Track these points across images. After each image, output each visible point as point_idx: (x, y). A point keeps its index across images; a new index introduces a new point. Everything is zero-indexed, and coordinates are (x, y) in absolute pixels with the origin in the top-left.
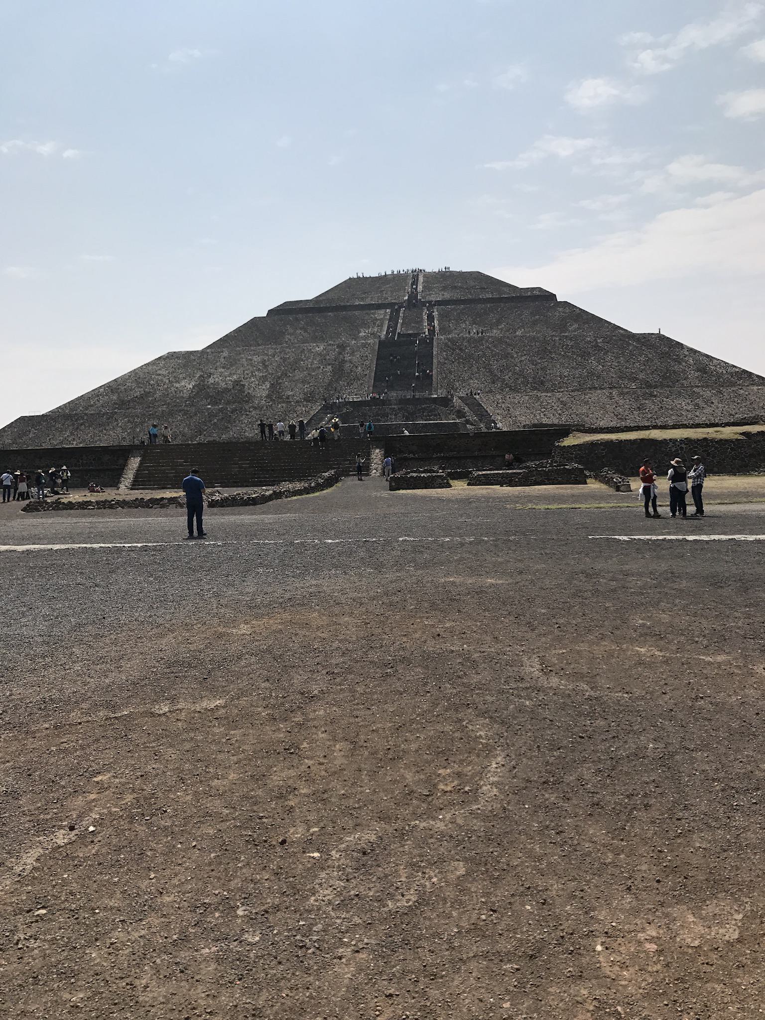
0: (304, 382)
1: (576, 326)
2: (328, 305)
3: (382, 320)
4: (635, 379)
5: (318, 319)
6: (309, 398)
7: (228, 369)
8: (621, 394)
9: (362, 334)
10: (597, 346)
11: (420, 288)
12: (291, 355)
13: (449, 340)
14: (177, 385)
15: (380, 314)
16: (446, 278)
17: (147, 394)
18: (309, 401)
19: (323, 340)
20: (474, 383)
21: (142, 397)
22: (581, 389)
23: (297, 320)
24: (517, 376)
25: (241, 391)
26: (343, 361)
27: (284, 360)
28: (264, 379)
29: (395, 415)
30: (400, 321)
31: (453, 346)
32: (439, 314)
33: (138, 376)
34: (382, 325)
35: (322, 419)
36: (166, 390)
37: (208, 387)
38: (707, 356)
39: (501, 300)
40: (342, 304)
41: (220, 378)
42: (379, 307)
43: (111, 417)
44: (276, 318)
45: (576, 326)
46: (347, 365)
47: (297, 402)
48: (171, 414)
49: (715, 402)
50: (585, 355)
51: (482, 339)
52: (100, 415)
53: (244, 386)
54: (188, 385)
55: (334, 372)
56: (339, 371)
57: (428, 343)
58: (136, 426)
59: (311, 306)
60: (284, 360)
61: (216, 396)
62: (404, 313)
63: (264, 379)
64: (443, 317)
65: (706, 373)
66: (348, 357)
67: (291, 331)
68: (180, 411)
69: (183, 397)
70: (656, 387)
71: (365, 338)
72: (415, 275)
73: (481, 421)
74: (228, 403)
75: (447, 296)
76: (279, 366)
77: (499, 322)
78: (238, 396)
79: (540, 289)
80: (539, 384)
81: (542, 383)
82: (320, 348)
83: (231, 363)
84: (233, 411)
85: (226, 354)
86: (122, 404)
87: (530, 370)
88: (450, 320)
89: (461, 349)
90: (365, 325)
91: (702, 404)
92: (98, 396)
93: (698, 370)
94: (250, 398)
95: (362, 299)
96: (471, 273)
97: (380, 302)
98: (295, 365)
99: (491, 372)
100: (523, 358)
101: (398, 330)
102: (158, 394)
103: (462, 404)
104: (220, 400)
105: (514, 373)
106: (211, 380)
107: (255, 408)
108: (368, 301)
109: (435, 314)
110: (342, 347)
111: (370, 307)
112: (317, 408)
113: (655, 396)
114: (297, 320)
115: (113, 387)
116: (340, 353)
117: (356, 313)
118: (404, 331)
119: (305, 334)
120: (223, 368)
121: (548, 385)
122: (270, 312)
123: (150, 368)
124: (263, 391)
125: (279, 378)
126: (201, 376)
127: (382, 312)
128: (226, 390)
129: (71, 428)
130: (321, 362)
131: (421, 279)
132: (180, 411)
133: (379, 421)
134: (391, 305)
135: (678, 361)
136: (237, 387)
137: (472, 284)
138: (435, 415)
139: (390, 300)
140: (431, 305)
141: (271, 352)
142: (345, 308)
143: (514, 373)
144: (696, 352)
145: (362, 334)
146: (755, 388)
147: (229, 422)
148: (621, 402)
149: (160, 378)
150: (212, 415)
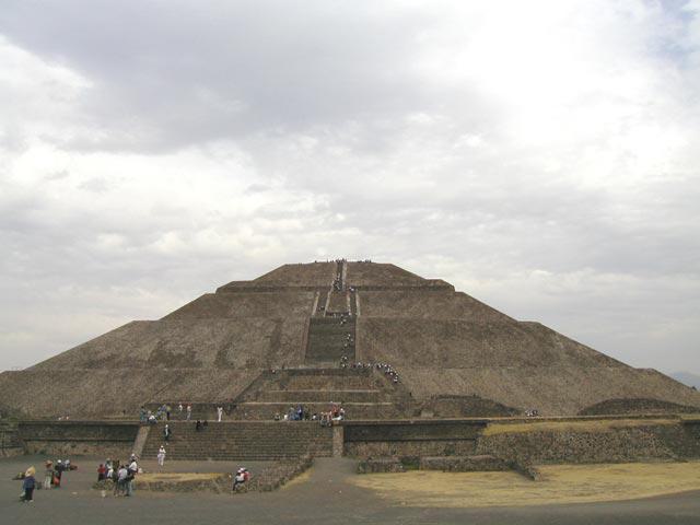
1: (470, 313)
3: (313, 301)
4: (519, 359)
6: (250, 365)
9: (296, 311)
11: (345, 274)
13: (369, 320)
15: (310, 295)
21: (109, 359)
25: (193, 357)
30: (328, 301)
31: (373, 326)
38: (575, 342)
42: (310, 289)
44: (224, 294)
49: (583, 379)
50: (479, 338)
51: (396, 321)
54: (147, 350)
56: (275, 343)
57: (353, 320)
58: (102, 385)
59: (254, 285)
61: (171, 360)
63: (212, 347)
66: (284, 331)
71: (298, 315)
72: (340, 263)
75: (367, 283)
77: (408, 306)
78: (190, 360)
79: (442, 281)
80: (446, 361)
81: (446, 360)
86: (92, 364)
91: (571, 379)
93: (567, 353)
94: (200, 364)
96: (385, 265)
108: (301, 284)
109: (357, 296)
110: (279, 321)
115: (86, 348)
121: (450, 361)
122: (219, 290)
124: (212, 357)
125: (226, 347)
128: (180, 356)
131: (345, 268)
133: (311, 388)
134: (317, 288)
135: (552, 345)
145: (296, 311)
146: (611, 370)
147: (181, 383)
150: (167, 377)
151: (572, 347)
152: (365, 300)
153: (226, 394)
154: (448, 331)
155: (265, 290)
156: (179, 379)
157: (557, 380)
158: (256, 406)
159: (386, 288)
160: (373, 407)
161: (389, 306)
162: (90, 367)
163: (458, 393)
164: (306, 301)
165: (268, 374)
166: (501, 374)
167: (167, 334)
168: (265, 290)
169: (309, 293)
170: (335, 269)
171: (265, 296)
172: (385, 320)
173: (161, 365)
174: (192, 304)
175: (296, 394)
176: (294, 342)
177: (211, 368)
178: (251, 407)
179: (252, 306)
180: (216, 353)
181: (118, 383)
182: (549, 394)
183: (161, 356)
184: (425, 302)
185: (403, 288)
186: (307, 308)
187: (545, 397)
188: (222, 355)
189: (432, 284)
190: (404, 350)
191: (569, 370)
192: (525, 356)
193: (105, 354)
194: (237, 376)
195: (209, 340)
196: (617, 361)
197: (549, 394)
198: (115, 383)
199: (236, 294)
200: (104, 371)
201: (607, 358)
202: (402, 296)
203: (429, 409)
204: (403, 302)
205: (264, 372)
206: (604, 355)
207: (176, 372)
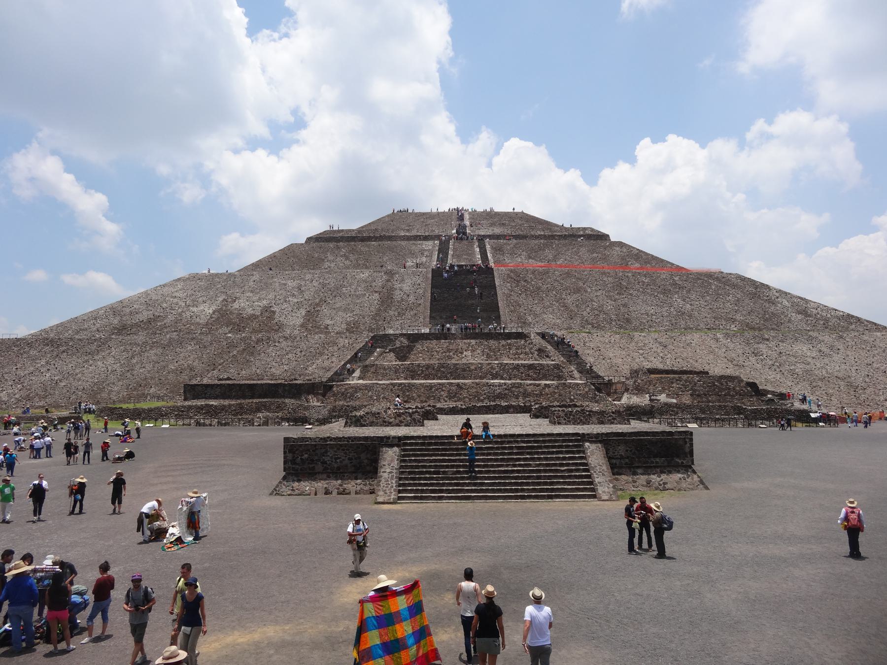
0: (345, 310)
2: (372, 235)
4: (734, 321)
5: (360, 246)
6: (352, 328)
7: (257, 293)
8: (727, 336)
9: (409, 264)
10: (675, 284)
12: (331, 282)
13: (511, 271)
14: (195, 309)
15: (428, 245)
16: (491, 216)
17: (156, 318)
18: (353, 332)
19: (367, 268)
20: (549, 317)
21: (149, 321)
22: (674, 326)
24: (596, 312)
25: (271, 317)
26: (392, 289)
27: (324, 285)
28: (299, 305)
29: (473, 351)
30: (451, 252)
31: (516, 277)
32: (492, 248)
33: (148, 300)
35: (371, 353)
36: (180, 315)
37: (231, 313)
39: (552, 237)
40: (387, 234)
41: (247, 304)
42: (426, 238)
43: (103, 344)
45: (637, 265)
46: (397, 292)
47: (337, 333)
48: (180, 343)
52: (91, 341)
53: (274, 312)
54: (206, 310)
55: (382, 302)
56: (387, 299)
58: (133, 357)
61: (239, 322)
62: (453, 245)
63: (299, 305)
64: (497, 250)
65: (810, 316)
66: (397, 286)
67: (331, 258)
68: (193, 339)
69: (198, 324)
70: (760, 330)
73: (570, 362)
74: (254, 331)
75: (497, 231)
76: (316, 292)
77: (555, 258)
78: (267, 323)
79: (592, 230)
80: (625, 323)
81: (628, 321)
82: (365, 274)
83: (264, 286)
84: (258, 341)
85: (256, 277)
86: (122, 329)
87: (609, 306)
88: (503, 255)
89: (525, 281)
90: (413, 254)
93: (800, 313)
94: (280, 327)
95: (408, 230)
97: (427, 234)
98: (336, 291)
99: (565, 306)
101: (449, 261)
102: (171, 318)
103: (544, 343)
104: (244, 328)
105: (593, 309)
106: (236, 305)
107: (286, 338)
108: (414, 233)
109: (488, 247)
110: (391, 274)
111: (416, 238)
112: (364, 338)
113: (768, 340)
114: (338, 248)
115: (115, 310)
116: (388, 281)
117: (403, 243)
118: (455, 262)
119: (348, 263)
121: (635, 323)
122: (309, 240)
123: (167, 288)
125: (317, 305)
127: (430, 243)
128: (253, 317)
129: (49, 356)
130: (367, 289)
131: (467, 216)
132: (193, 339)
133: (450, 358)
134: (438, 237)
136: (267, 314)
137: (520, 222)
138: (526, 353)
139: (437, 232)
140: (481, 239)
141: (308, 277)
142: (390, 238)
143: (593, 309)
144: (786, 293)
147: (252, 354)
148: (731, 346)
149: (175, 300)
150: (231, 345)
151: (802, 307)
153: (318, 370)
154: (620, 287)
155: (369, 239)
156: (250, 350)
157: (802, 348)
158: (366, 386)
159: (524, 237)
160: (557, 387)
161: (530, 258)
162: (116, 334)
163: (661, 366)
164: (422, 252)
165: (380, 341)
166: (717, 340)
167: (237, 292)
168: (369, 239)
170: (455, 217)
171: (368, 246)
172: (533, 272)
173: (225, 329)
174: (273, 257)
175: (428, 367)
176: (412, 299)
177: (296, 332)
178: (357, 388)
179: (352, 257)
180: (303, 312)
181: (156, 354)
182: (799, 368)
183: (223, 317)
184: (577, 253)
185: (545, 237)
186: (424, 259)
187: (792, 373)
189: (581, 233)
191: (814, 334)
192: (738, 317)
193: (145, 316)
194: (335, 344)
195: (294, 295)
196: (875, 324)
197: (799, 368)
198: (152, 354)
199: (331, 245)
200: (141, 337)
201: (859, 320)
202: (546, 246)
203: (639, 390)
204: (549, 253)
205: (372, 337)
206: (853, 316)
207: (243, 339)
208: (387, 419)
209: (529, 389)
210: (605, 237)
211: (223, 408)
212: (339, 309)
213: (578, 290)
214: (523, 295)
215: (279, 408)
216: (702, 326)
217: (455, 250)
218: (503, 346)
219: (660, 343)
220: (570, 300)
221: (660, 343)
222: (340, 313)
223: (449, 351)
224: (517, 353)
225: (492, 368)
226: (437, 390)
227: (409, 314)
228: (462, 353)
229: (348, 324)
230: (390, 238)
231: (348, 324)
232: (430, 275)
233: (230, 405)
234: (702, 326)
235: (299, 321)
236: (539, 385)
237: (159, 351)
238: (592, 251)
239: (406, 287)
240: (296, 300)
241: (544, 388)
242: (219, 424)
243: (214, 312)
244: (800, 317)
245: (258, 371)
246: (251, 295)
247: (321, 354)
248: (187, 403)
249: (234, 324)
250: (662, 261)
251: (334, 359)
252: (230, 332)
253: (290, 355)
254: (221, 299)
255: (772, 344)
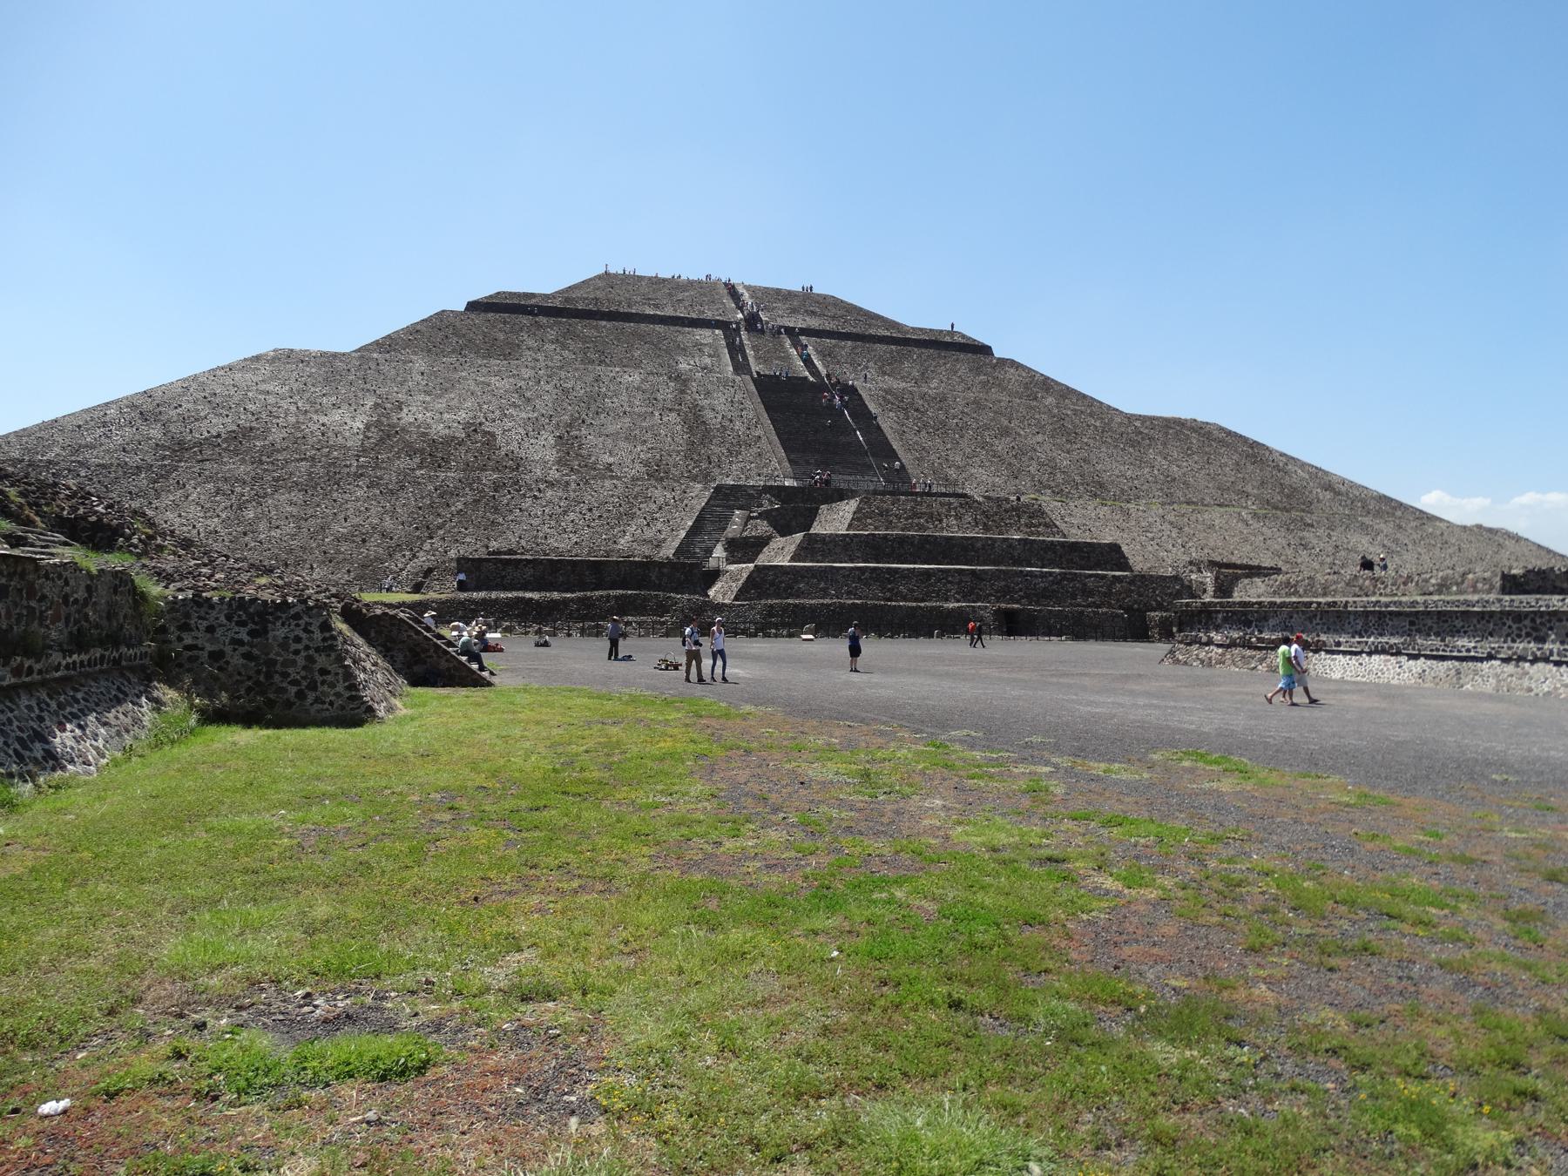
6: (657, 472)
14: (323, 419)
15: (704, 335)
23: (539, 326)
26: (696, 410)
28: (535, 427)
29: (958, 517)
33: (205, 390)
34: (715, 355)
36: (297, 426)
41: (432, 413)
44: (490, 315)
46: (709, 414)
47: (633, 479)
53: (493, 435)
54: (349, 422)
60: (566, 391)
67: (531, 343)
75: (814, 323)
77: (924, 377)
79: (964, 336)
81: (1101, 485)
89: (917, 410)
90: (684, 351)
92: (104, 424)
94: (518, 464)
95: (656, 306)
97: (694, 316)
100: (1040, 438)
114: (539, 326)
117: (657, 327)
120: (428, 393)
122: (473, 306)
124: (542, 451)
126: (376, 405)
127: (707, 332)
128: (449, 441)
136: (479, 437)
139: (709, 315)
140: (790, 331)
142: (628, 317)
147: (496, 510)
148: (1268, 533)
152: (823, 355)
161: (884, 373)
164: (699, 346)
169: (698, 331)
171: (596, 328)
174: (413, 330)
175: (902, 540)
177: (554, 474)
186: (708, 361)
188: (568, 445)
189: (947, 339)
190: (1002, 460)
195: (514, 405)
199: (525, 320)
208: (1558, 584)
209: (1090, 583)
210: (986, 350)
211: (554, 604)
212: (615, 436)
213: (1005, 432)
214: (923, 433)
215: (662, 609)
216: (1208, 500)
217: (755, 348)
218: (1006, 511)
219: (1171, 523)
220: (1001, 446)
221: (1171, 523)
222: (622, 444)
223: (916, 515)
224: (1032, 525)
225: (1010, 546)
226: (939, 580)
227: (748, 454)
228: (941, 521)
229: (646, 464)
230: (628, 317)
231: (646, 464)
232: (753, 388)
233: (565, 602)
234: (1208, 500)
235: (551, 455)
236: (1104, 577)
237: (297, 496)
238: (977, 371)
239: (720, 400)
240: (524, 415)
241: (1113, 583)
242: (583, 632)
243: (368, 427)
244: (1328, 495)
245: (523, 543)
246: (428, 399)
247: (633, 516)
248: (463, 596)
249: (422, 451)
250: (1084, 396)
251: (659, 526)
252: (420, 468)
253: (572, 516)
254: (370, 402)
255: (1320, 532)
